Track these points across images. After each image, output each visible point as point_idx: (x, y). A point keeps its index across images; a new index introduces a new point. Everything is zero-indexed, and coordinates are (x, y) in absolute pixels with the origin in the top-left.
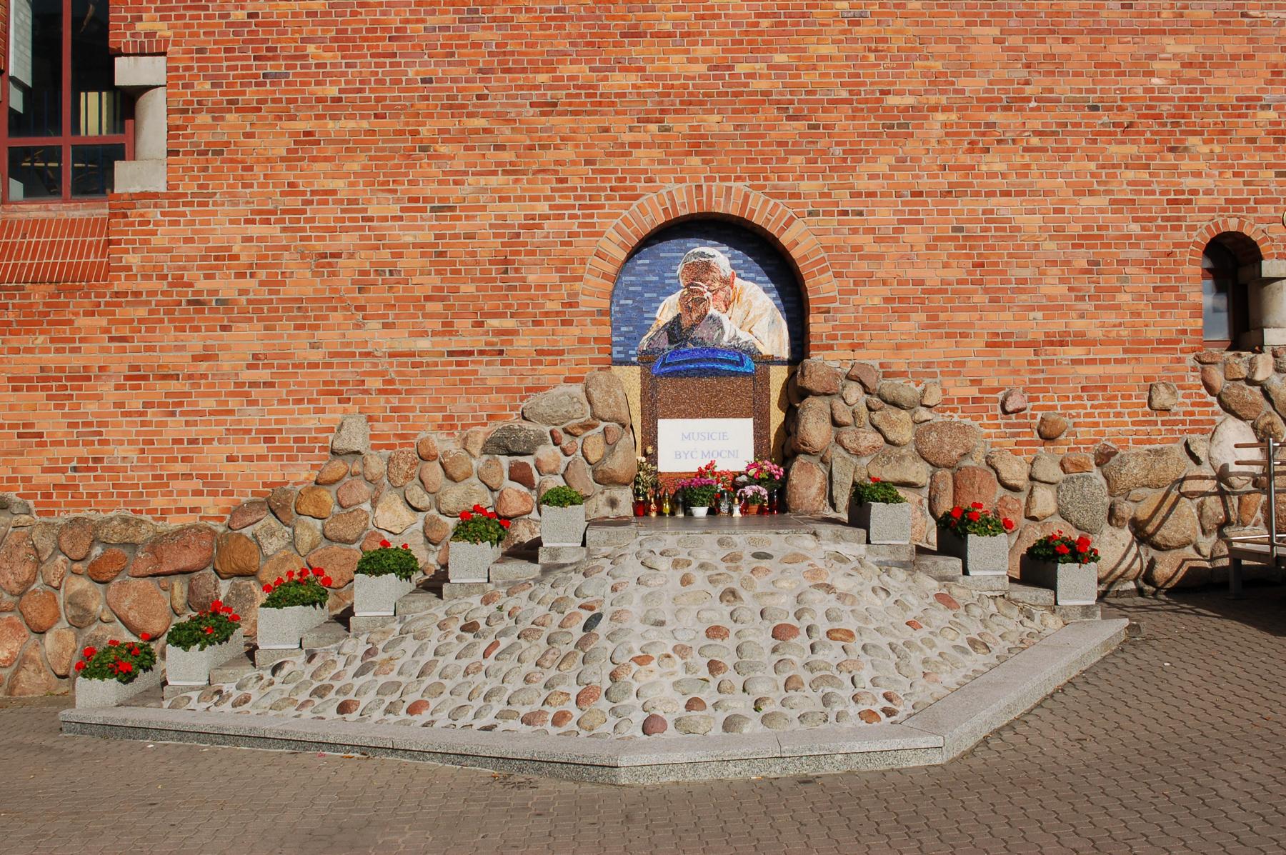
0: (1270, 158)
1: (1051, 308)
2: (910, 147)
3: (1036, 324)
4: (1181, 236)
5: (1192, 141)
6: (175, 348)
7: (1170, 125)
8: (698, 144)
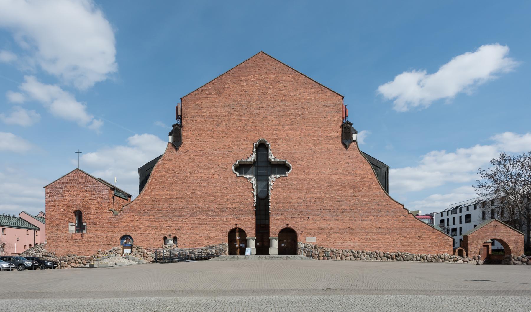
6: (87, 244)
7: (161, 228)
8: (126, 230)
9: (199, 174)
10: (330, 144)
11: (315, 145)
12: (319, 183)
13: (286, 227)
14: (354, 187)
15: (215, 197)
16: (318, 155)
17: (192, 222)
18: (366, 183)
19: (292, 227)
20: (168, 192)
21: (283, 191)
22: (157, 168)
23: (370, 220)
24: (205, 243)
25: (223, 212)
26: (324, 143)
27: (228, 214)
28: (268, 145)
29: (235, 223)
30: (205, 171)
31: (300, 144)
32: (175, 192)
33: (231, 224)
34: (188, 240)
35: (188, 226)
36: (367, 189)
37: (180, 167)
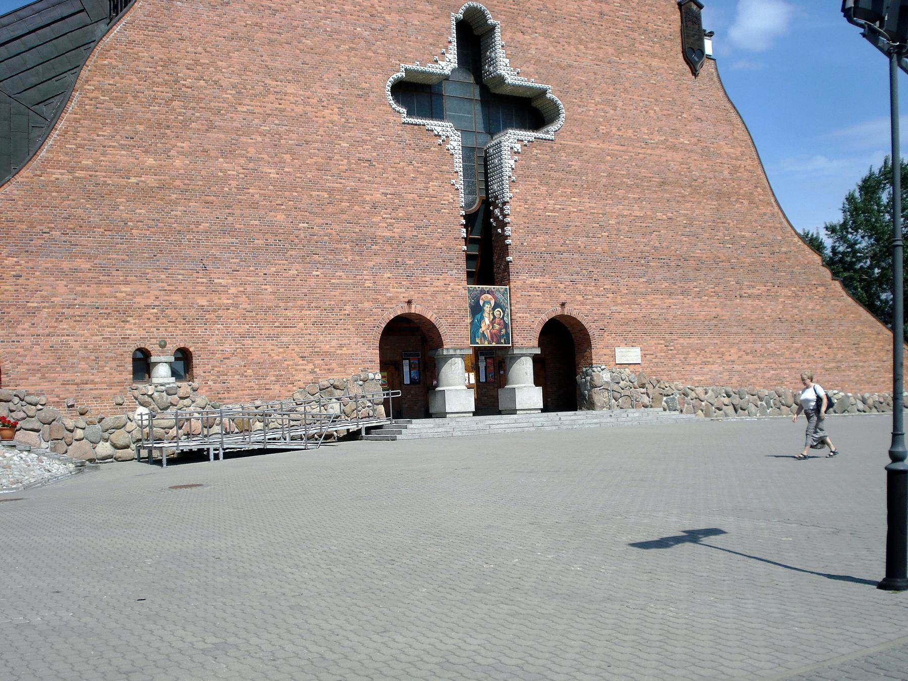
0: (154, 324)
1: (83, 372)
2: (35, 320)
3: (78, 378)
4: (126, 349)
5: (129, 319)
7: (124, 313)
9: (272, 97)
10: (654, 56)
11: (619, 51)
12: (636, 171)
13: (559, 311)
14: (719, 195)
15: (331, 191)
16: (627, 85)
17: (249, 289)
18: (743, 183)
19: (574, 314)
20: (150, 161)
21: (543, 189)
22: (103, 56)
23: (759, 297)
24: (300, 376)
25: (360, 254)
26: (641, 47)
27: (378, 259)
28: (493, 27)
29: (404, 295)
30: (291, 88)
31: (581, 41)
32: (178, 163)
33: (390, 299)
34: (236, 361)
35: (236, 306)
36: (746, 202)
37: (197, 62)
